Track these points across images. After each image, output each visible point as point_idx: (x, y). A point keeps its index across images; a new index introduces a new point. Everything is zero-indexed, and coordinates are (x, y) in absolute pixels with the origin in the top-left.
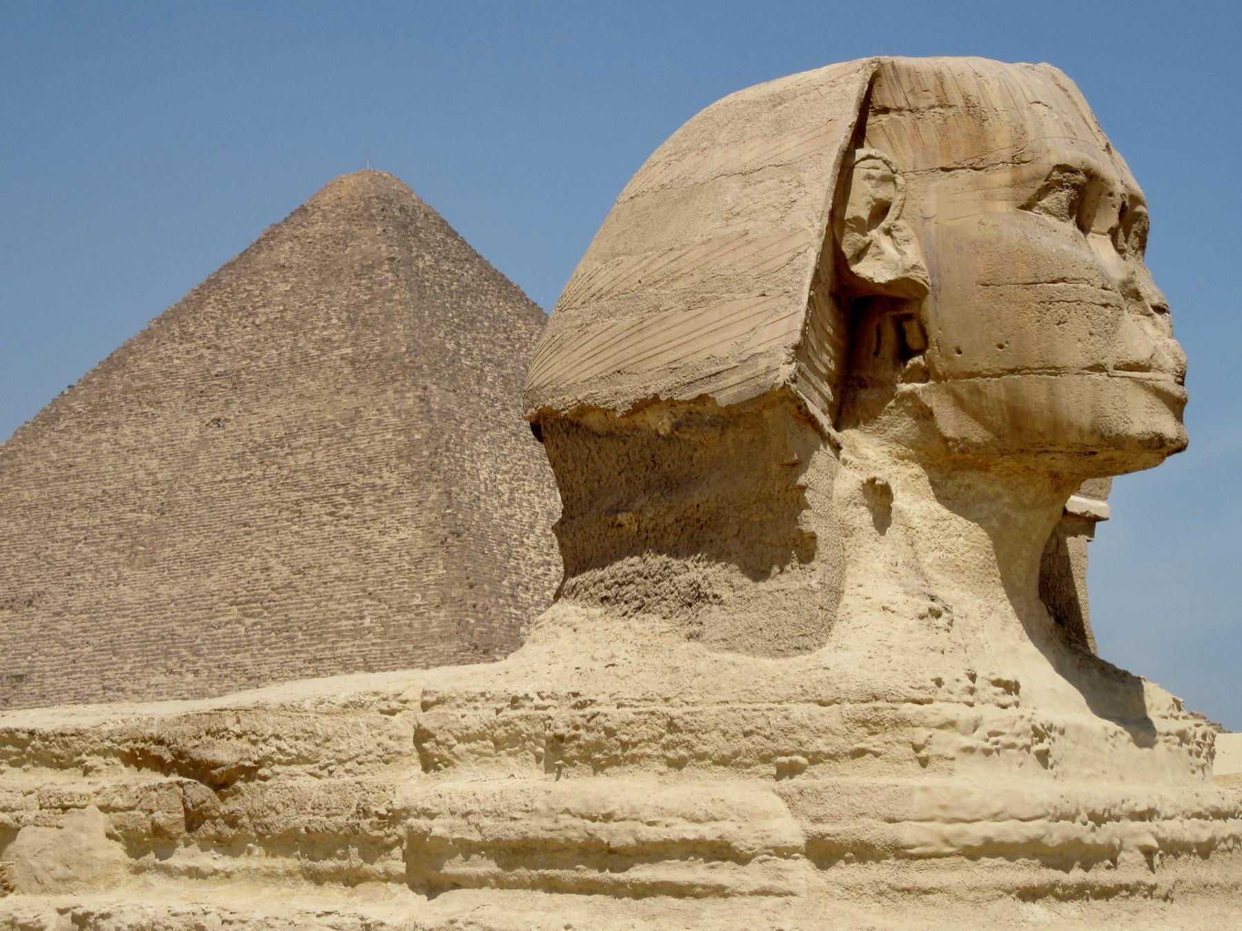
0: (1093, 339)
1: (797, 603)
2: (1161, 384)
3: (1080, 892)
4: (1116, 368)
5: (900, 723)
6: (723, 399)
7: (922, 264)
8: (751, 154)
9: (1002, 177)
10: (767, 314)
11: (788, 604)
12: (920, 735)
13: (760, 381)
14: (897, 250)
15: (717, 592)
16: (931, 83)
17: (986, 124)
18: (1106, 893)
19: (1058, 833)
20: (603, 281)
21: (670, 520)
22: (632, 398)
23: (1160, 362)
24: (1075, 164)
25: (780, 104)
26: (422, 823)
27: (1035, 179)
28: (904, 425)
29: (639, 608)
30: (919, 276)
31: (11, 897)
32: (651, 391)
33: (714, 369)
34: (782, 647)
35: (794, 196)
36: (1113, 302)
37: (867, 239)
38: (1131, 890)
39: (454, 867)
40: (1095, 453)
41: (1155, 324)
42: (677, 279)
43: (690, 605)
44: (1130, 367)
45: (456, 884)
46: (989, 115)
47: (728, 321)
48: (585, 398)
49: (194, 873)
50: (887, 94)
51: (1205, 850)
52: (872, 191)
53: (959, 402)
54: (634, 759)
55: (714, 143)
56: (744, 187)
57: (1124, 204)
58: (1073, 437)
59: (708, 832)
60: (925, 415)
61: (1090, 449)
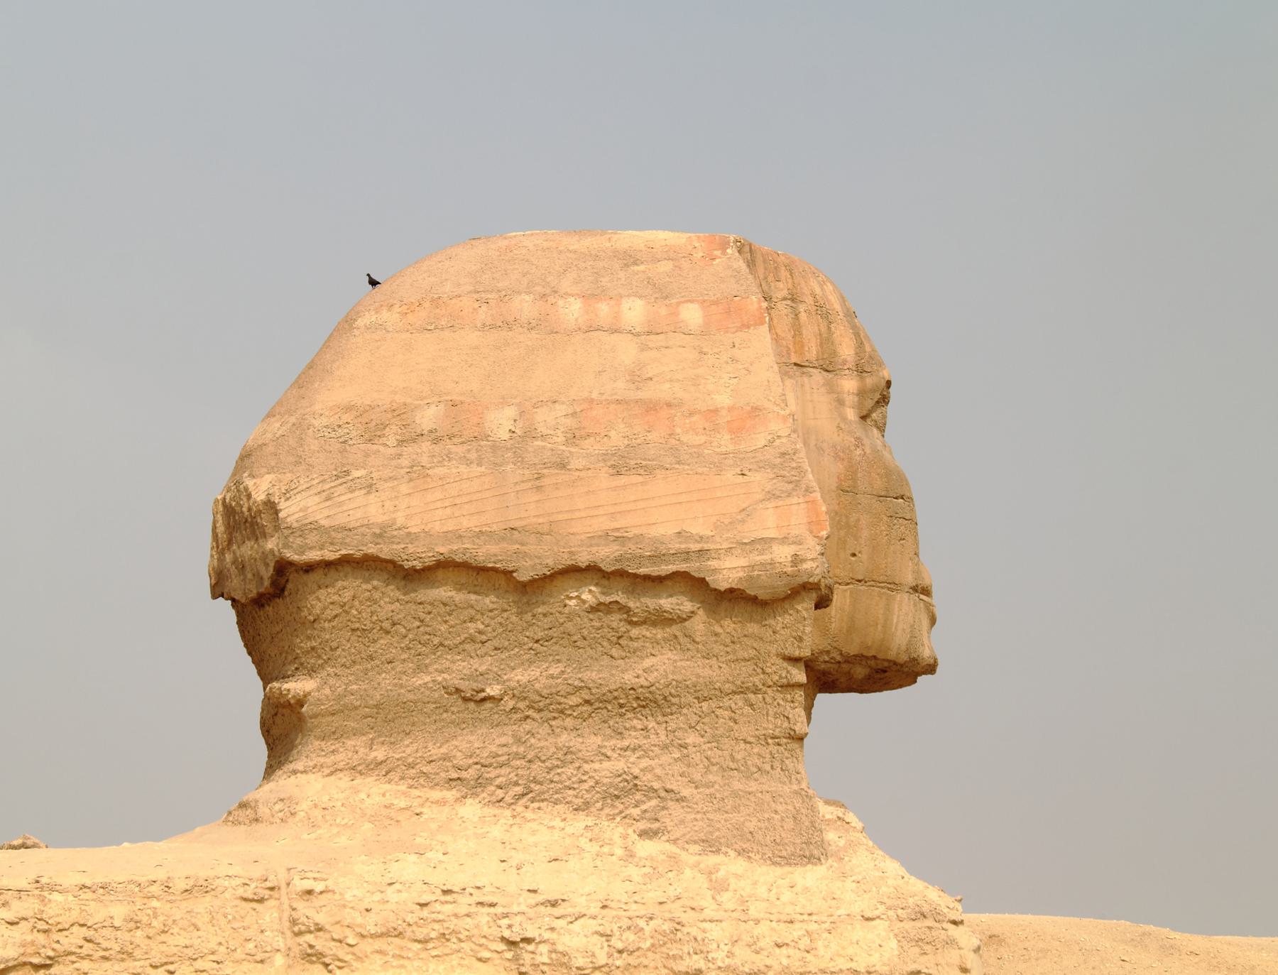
9: (849, 384)
10: (759, 497)
11: (780, 808)
13: (789, 570)
15: (669, 786)
16: (784, 273)
20: (428, 418)
21: (574, 700)
22: (550, 562)
25: (635, 263)
33: (697, 547)
34: (784, 853)
43: (617, 797)
48: (451, 551)
56: (642, 350)
58: (892, 655)
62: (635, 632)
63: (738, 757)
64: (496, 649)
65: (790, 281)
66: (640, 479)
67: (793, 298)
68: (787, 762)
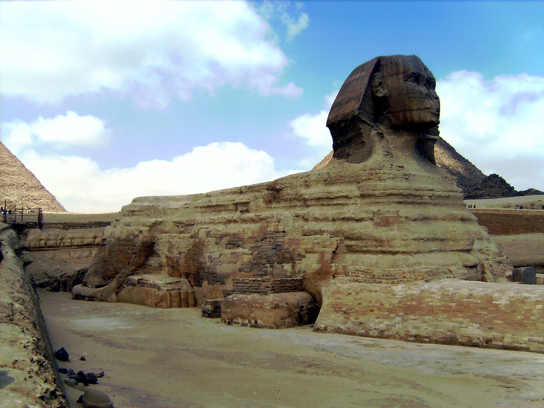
3: (412, 203)
5: (376, 173)
6: (349, 119)
8: (358, 76)
9: (401, 76)
12: (379, 176)
16: (389, 60)
18: (419, 203)
19: (406, 192)
26: (305, 196)
27: (407, 75)
28: (387, 122)
30: (388, 95)
31: (249, 214)
38: (425, 203)
39: (309, 203)
44: (426, 109)
45: (310, 206)
49: (275, 208)
51: (448, 197)
54: (336, 183)
59: (344, 194)
60: (390, 120)
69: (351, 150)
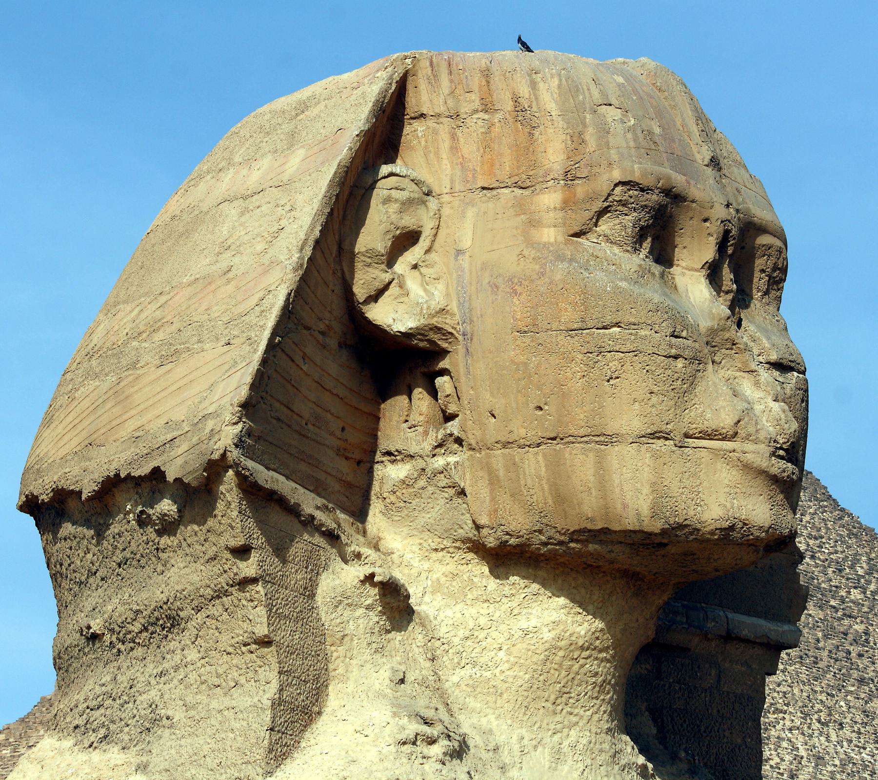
0: (654, 399)
1: (245, 724)
2: (749, 457)
4: (687, 436)
7: (454, 307)
9: (550, 199)
10: (226, 367)
11: (236, 725)
14: (425, 290)
15: (170, 713)
16: (476, 82)
17: (536, 133)
21: (137, 627)
23: (751, 429)
24: (645, 183)
29: (105, 737)
32: (114, 465)
33: (169, 437)
35: (283, 223)
36: (687, 353)
37: (387, 277)
40: (665, 545)
41: (757, 384)
42: (159, 329)
46: (542, 120)
47: (191, 377)
50: (424, 97)
52: (394, 217)
53: (494, 481)
55: (230, 163)
56: (242, 214)
57: (727, 233)
58: (630, 523)
61: (658, 540)
62: (165, 541)
63: (220, 671)
64: (103, 579)
65: (485, 89)
66: (170, 366)
67: (487, 107)
68: (260, 671)
69: (173, 690)
